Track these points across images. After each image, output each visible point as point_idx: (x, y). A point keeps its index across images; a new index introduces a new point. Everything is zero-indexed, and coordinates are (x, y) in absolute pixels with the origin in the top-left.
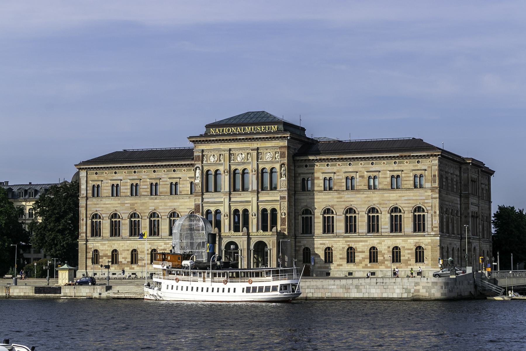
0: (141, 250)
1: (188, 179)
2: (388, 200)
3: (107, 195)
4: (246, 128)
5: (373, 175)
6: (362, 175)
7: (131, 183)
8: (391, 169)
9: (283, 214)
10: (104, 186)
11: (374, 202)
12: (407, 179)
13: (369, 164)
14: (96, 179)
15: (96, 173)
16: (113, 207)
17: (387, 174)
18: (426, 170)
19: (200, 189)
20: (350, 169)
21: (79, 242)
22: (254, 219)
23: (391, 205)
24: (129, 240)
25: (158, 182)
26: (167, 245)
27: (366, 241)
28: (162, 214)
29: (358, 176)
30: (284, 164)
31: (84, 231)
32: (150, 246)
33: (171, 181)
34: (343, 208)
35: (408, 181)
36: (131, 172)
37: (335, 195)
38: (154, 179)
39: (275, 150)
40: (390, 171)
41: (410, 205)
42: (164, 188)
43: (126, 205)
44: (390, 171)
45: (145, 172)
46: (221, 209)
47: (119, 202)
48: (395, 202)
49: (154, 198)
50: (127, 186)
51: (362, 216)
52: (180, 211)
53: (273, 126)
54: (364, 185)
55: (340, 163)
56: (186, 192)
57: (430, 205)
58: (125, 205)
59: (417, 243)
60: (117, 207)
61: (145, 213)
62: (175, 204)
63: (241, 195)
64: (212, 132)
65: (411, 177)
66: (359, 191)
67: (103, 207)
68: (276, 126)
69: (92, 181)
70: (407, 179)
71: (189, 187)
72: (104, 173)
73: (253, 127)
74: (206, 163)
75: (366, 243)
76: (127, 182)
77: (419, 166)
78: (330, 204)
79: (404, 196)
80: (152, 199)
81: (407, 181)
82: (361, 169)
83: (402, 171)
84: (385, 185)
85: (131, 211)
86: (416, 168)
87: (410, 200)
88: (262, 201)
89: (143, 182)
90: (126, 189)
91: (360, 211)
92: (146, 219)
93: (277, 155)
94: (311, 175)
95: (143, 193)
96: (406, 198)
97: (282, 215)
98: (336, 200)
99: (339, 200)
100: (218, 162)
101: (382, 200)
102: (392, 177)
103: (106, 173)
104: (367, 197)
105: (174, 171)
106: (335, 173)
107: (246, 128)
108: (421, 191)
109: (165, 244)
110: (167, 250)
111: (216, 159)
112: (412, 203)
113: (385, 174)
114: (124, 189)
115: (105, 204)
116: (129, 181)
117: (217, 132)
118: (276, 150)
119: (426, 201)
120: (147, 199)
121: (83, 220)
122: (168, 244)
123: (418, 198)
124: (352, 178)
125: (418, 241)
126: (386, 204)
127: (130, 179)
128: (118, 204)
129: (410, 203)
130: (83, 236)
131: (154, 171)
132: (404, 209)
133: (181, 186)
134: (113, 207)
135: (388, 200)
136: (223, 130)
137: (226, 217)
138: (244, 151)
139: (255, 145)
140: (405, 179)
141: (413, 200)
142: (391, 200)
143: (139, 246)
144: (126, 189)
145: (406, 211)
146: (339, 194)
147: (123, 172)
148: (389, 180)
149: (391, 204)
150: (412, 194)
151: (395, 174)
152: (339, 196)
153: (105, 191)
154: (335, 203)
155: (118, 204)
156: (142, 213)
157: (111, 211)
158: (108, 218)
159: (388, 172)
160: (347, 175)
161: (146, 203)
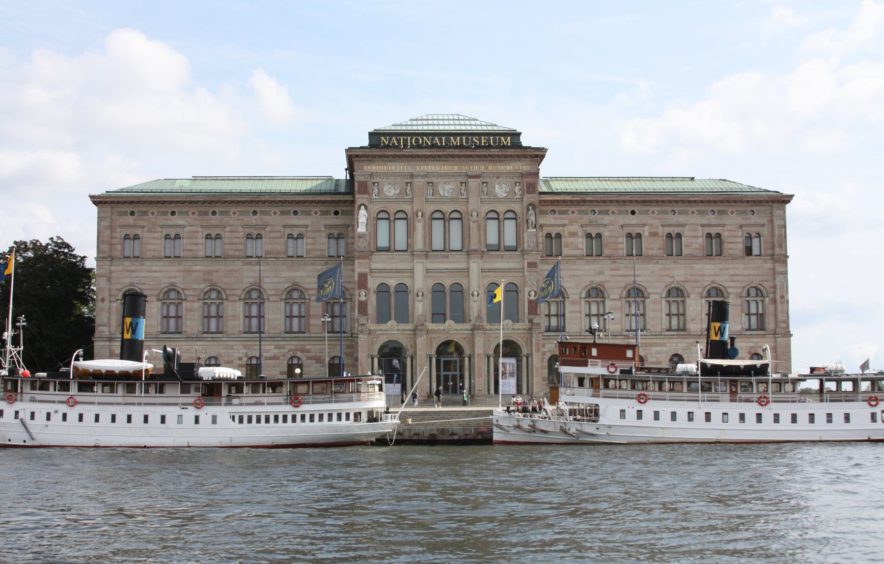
0: (226, 358)
1: (323, 229)
2: (701, 275)
3: (156, 254)
4: (452, 138)
5: (674, 232)
6: (654, 230)
7: (205, 233)
8: (705, 221)
9: (533, 293)
10: (148, 238)
11: (677, 278)
12: (734, 240)
13: (666, 212)
14: (132, 224)
15: (132, 213)
16: (168, 277)
17: (698, 230)
18: (763, 225)
19: (366, 244)
20: (633, 220)
21: (96, 344)
22: (475, 301)
23: (706, 284)
24: (198, 339)
25: (262, 233)
26: (282, 350)
27: (664, 345)
28: (269, 292)
29: (646, 234)
30: (530, 204)
31: (105, 320)
32: (246, 351)
33: (288, 231)
34: (620, 288)
35: (736, 245)
36: (206, 213)
37: (605, 265)
38: (255, 226)
39: (515, 179)
40: (702, 226)
41: (739, 284)
42: (273, 244)
43: (197, 274)
44: (702, 226)
45: (234, 213)
46: (407, 281)
47: (181, 268)
48: (712, 278)
49: (254, 263)
50: (197, 238)
51: (654, 302)
52: (307, 286)
53: (502, 138)
54: (659, 249)
55: (615, 209)
56: (319, 253)
57: (771, 284)
58: (191, 275)
59: (751, 347)
60: (174, 277)
61: (234, 289)
62: (297, 274)
63: (447, 257)
64: (384, 142)
65: (739, 237)
66: (650, 258)
67: (145, 277)
68: (509, 138)
69: (122, 226)
70: (734, 240)
71: (325, 244)
72: (149, 213)
73: (464, 138)
74: (377, 197)
75: (664, 349)
76: (197, 232)
77: (754, 219)
78: (599, 279)
79: (728, 269)
80: (249, 263)
81: (732, 243)
82: (651, 221)
83: (724, 226)
84: (696, 249)
85: (204, 286)
86: (747, 222)
87: (738, 275)
88: (490, 270)
89: (231, 232)
90: (195, 244)
91: (653, 293)
92: (235, 301)
93: (517, 188)
94: (562, 228)
95: (230, 253)
96: (731, 272)
97: (530, 296)
98: (607, 273)
99: (614, 273)
100: (401, 197)
101: (691, 275)
102: (709, 236)
103: (153, 214)
104: (664, 269)
105: (296, 213)
106: (605, 225)
107: (452, 138)
108: (758, 262)
109: (277, 347)
110: (281, 358)
111: (398, 191)
112: (742, 281)
113: (695, 231)
114: (190, 244)
115: (149, 271)
116: (200, 229)
117: (394, 144)
118: (515, 180)
119: (766, 278)
120: (239, 264)
121: (103, 300)
122: (282, 347)
123: (752, 272)
124: (639, 236)
125: (753, 345)
126: (698, 281)
127: (202, 227)
128: (179, 271)
129: (738, 281)
130: (103, 332)
131: (255, 213)
132: (729, 290)
133: (309, 241)
134: (171, 277)
135: (701, 275)
136: (405, 141)
137: (420, 297)
138: (453, 179)
139: (476, 168)
140: (729, 240)
141: (743, 275)
142: (705, 275)
143: (222, 351)
144: (195, 244)
145: (733, 293)
146: (614, 262)
147: (188, 212)
148: (700, 240)
149: (707, 282)
150: (742, 266)
151: (714, 231)
152: (613, 266)
153: (150, 247)
154: (607, 278)
155: (179, 271)
156: (227, 289)
157: (165, 282)
158: (155, 298)
159: (700, 228)
160: (627, 230)
161: (237, 271)
